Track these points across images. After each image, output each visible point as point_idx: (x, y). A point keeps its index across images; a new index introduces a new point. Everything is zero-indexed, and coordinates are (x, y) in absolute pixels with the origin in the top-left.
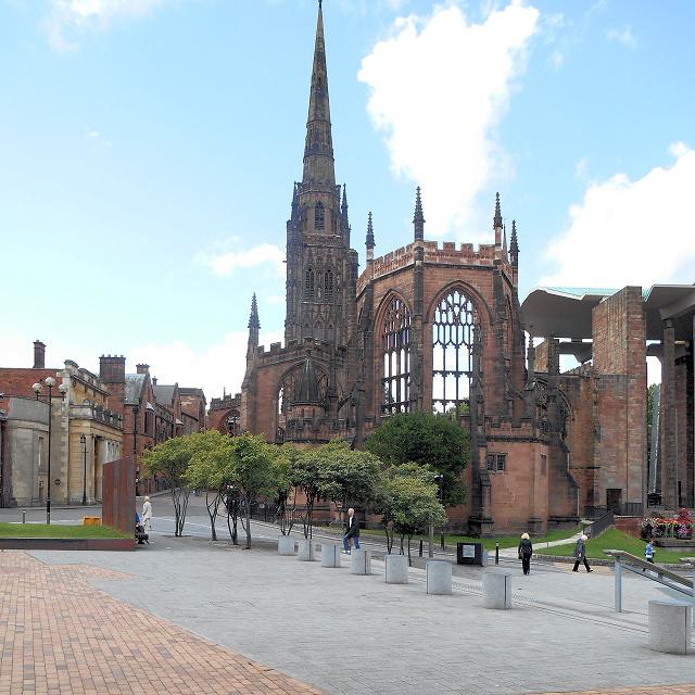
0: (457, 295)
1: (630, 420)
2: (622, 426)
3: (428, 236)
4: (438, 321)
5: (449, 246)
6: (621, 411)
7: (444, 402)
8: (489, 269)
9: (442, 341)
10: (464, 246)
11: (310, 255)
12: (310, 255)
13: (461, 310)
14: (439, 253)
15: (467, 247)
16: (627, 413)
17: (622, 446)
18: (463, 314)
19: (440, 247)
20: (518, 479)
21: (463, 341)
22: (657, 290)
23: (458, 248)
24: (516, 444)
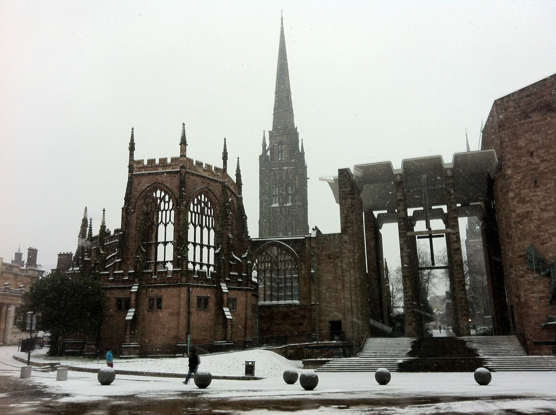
0: (158, 192)
1: (345, 266)
2: (339, 271)
3: (136, 158)
4: (192, 210)
5: (151, 162)
6: (338, 260)
7: (194, 264)
8: (177, 172)
9: (164, 222)
10: (160, 160)
11: (275, 175)
12: (275, 175)
13: (161, 202)
14: (145, 167)
15: (163, 161)
16: (341, 262)
17: (339, 287)
18: (163, 203)
19: (146, 163)
20: (171, 314)
21: (162, 221)
22: (406, 163)
23: (157, 162)
24: (169, 289)
